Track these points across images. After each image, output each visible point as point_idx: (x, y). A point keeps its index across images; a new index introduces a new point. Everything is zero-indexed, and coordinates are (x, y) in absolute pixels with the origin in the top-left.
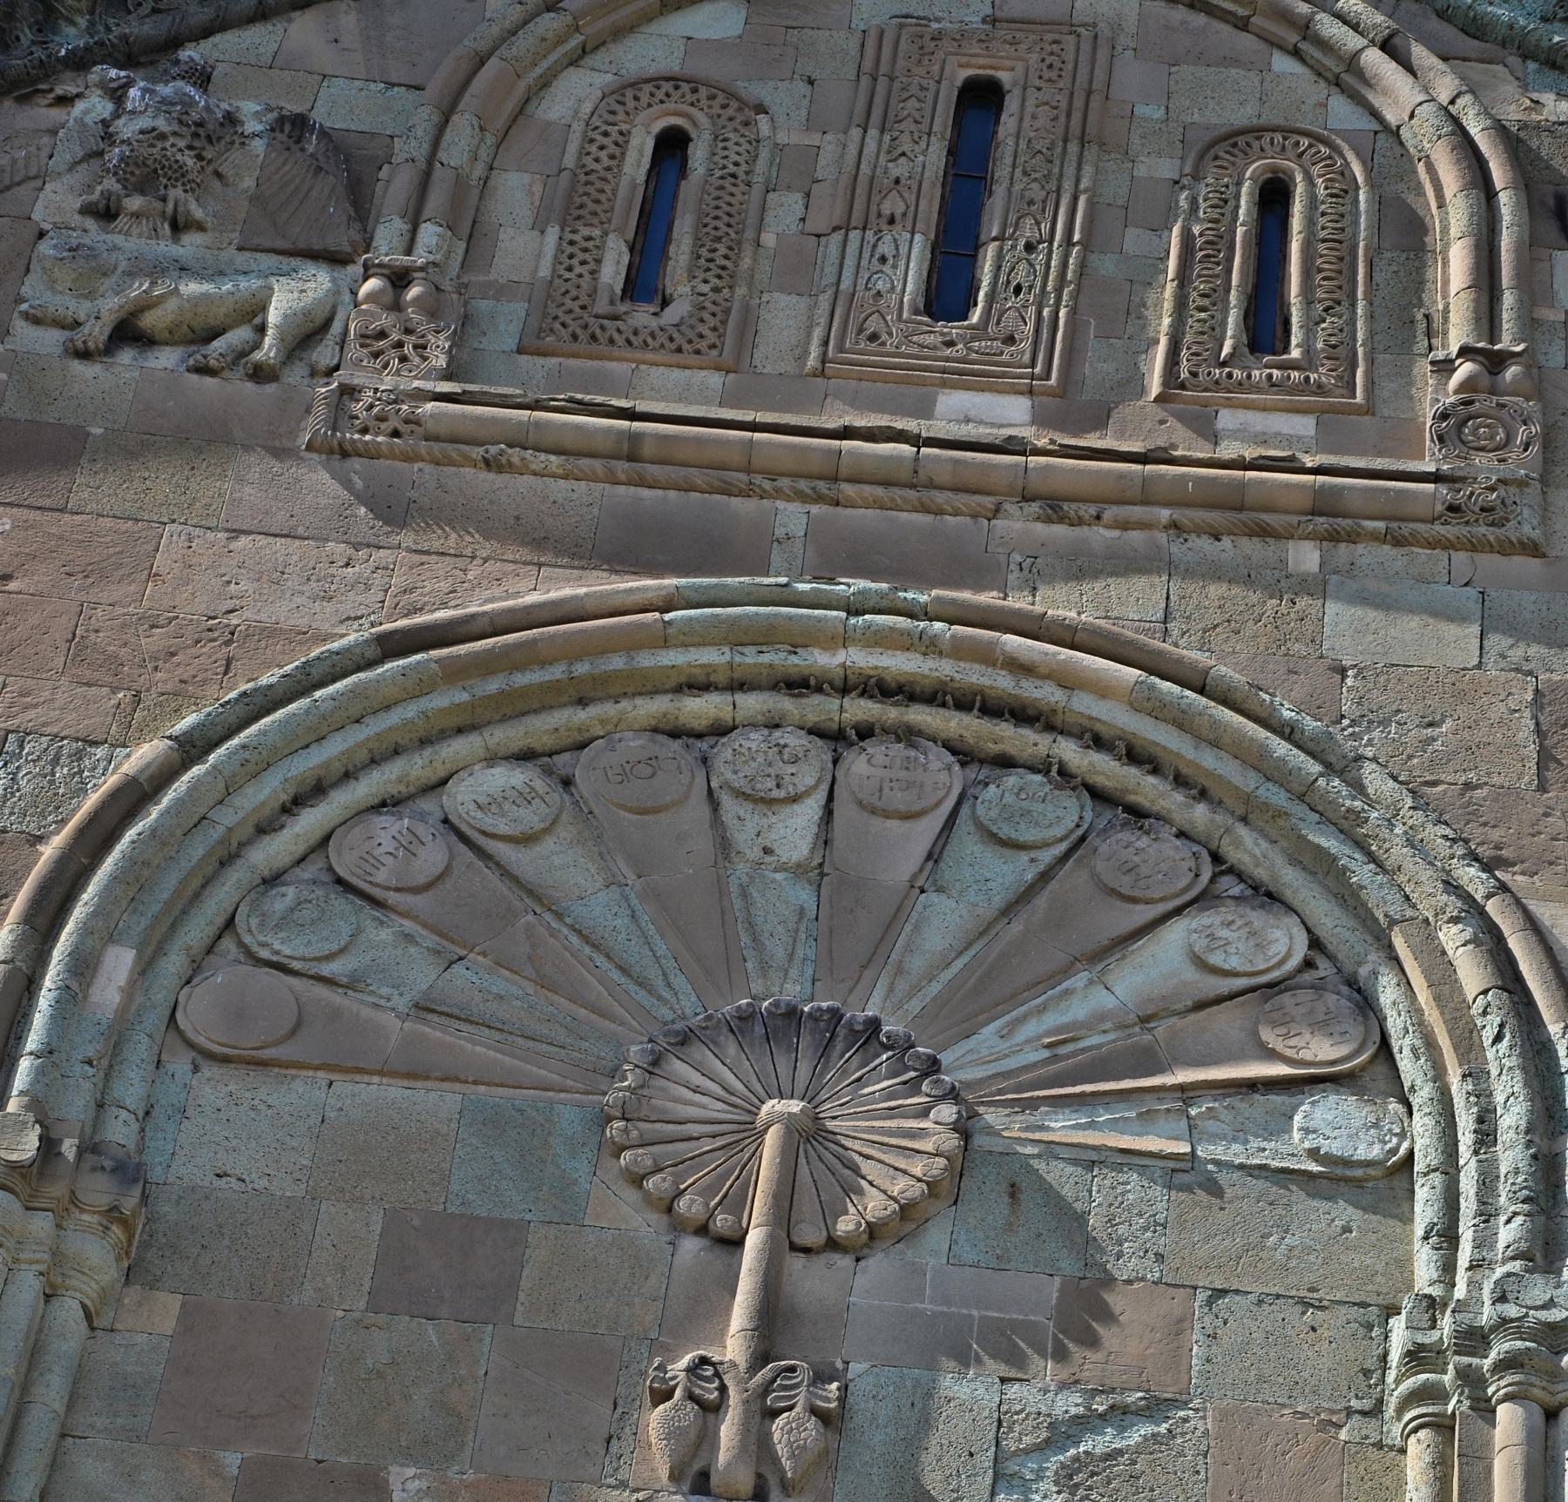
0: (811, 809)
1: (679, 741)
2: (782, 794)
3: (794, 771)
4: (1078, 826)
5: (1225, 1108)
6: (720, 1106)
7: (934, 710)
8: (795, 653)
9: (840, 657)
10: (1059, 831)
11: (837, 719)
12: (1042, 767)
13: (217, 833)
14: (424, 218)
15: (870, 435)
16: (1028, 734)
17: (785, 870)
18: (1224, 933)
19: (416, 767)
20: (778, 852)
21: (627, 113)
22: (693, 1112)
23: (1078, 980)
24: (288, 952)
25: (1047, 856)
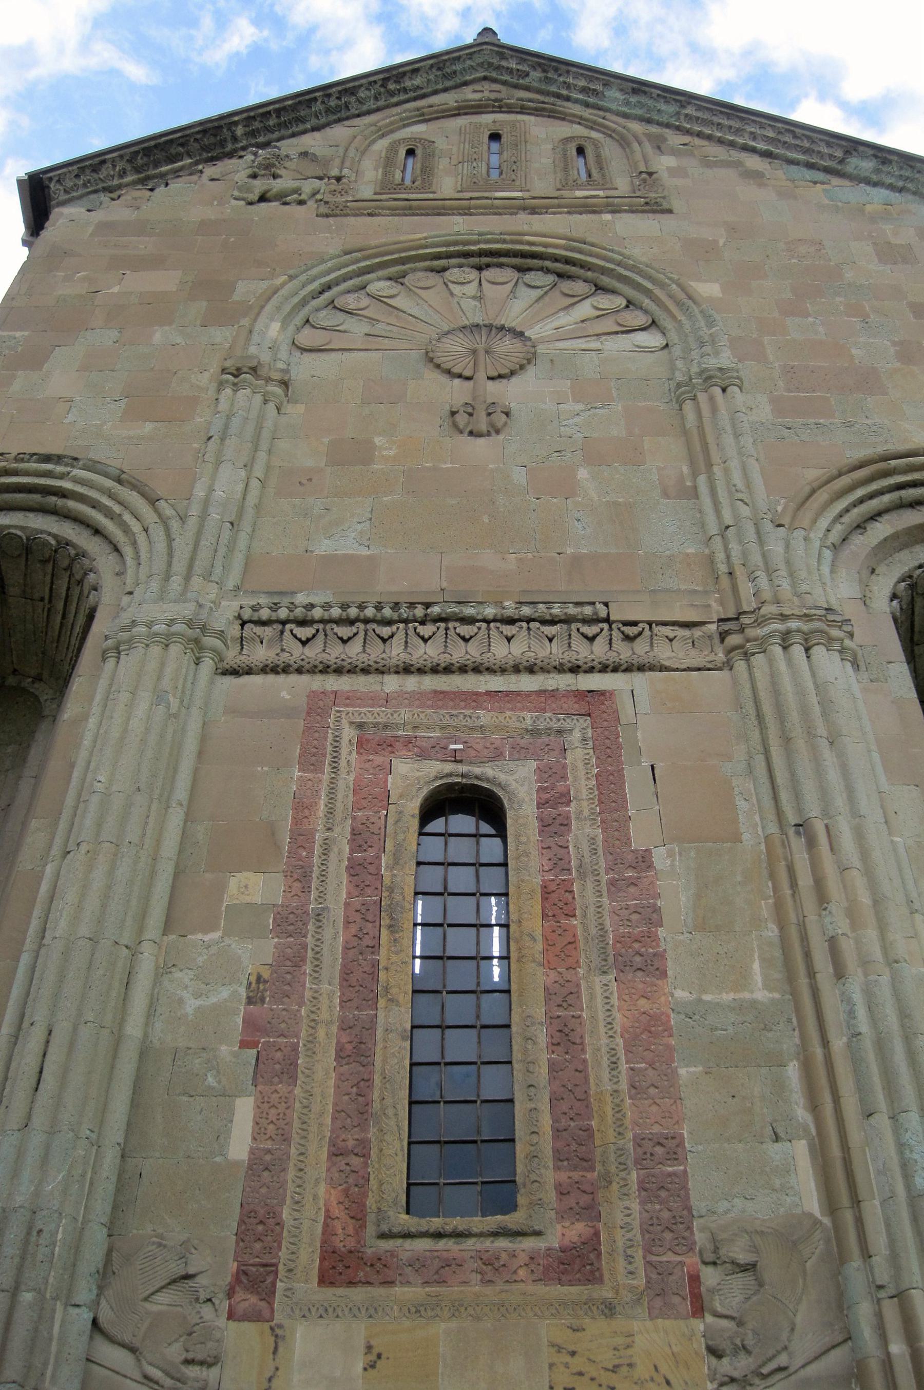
0: (476, 283)
9: (478, 247)
12: (541, 269)
15: (477, 198)
16: (535, 261)
25: (545, 289)
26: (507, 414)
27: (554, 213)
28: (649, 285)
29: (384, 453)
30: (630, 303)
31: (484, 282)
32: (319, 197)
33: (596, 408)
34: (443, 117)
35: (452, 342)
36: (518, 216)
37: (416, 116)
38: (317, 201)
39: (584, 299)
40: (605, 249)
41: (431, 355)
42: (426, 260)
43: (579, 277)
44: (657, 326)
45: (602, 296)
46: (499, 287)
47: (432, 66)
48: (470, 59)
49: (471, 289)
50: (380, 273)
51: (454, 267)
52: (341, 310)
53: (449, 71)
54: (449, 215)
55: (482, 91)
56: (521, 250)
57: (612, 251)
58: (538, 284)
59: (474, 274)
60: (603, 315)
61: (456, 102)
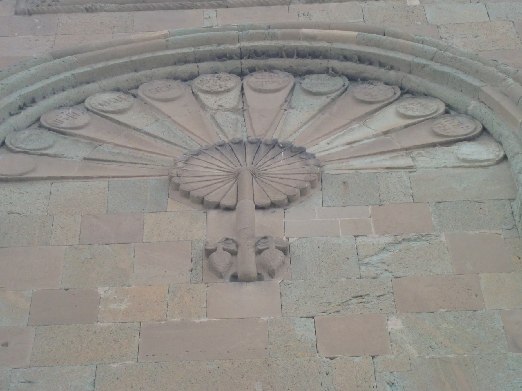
0: (236, 92)
2: (223, 89)
3: (226, 83)
4: (344, 86)
7: (278, 59)
8: (219, 46)
9: (238, 45)
10: (337, 88)
11: (240, 67)
12: (326, 71)
16: (318, 61)
17: (228, 111)
18: (411, 106)
19: (71, 94)
20: (224, 106)
25: (333, 96)
26: (285, 251)
28: (476, 83)
29: (113, 306)
30: (449, 109)
31: (247, 91)
33: (409, 240)
35: (205, 165)
40: (413, 40)
41: (176, 180)
42: (166, 65)
43: (377, 79)
44: (489, 133)
46: (271, 96)
50: (104, 83)
52: (50, 130)
54: (197, 8)
56: (296, 48)
58: (322, 89)
59: (233, 82)
60: (414, 124)
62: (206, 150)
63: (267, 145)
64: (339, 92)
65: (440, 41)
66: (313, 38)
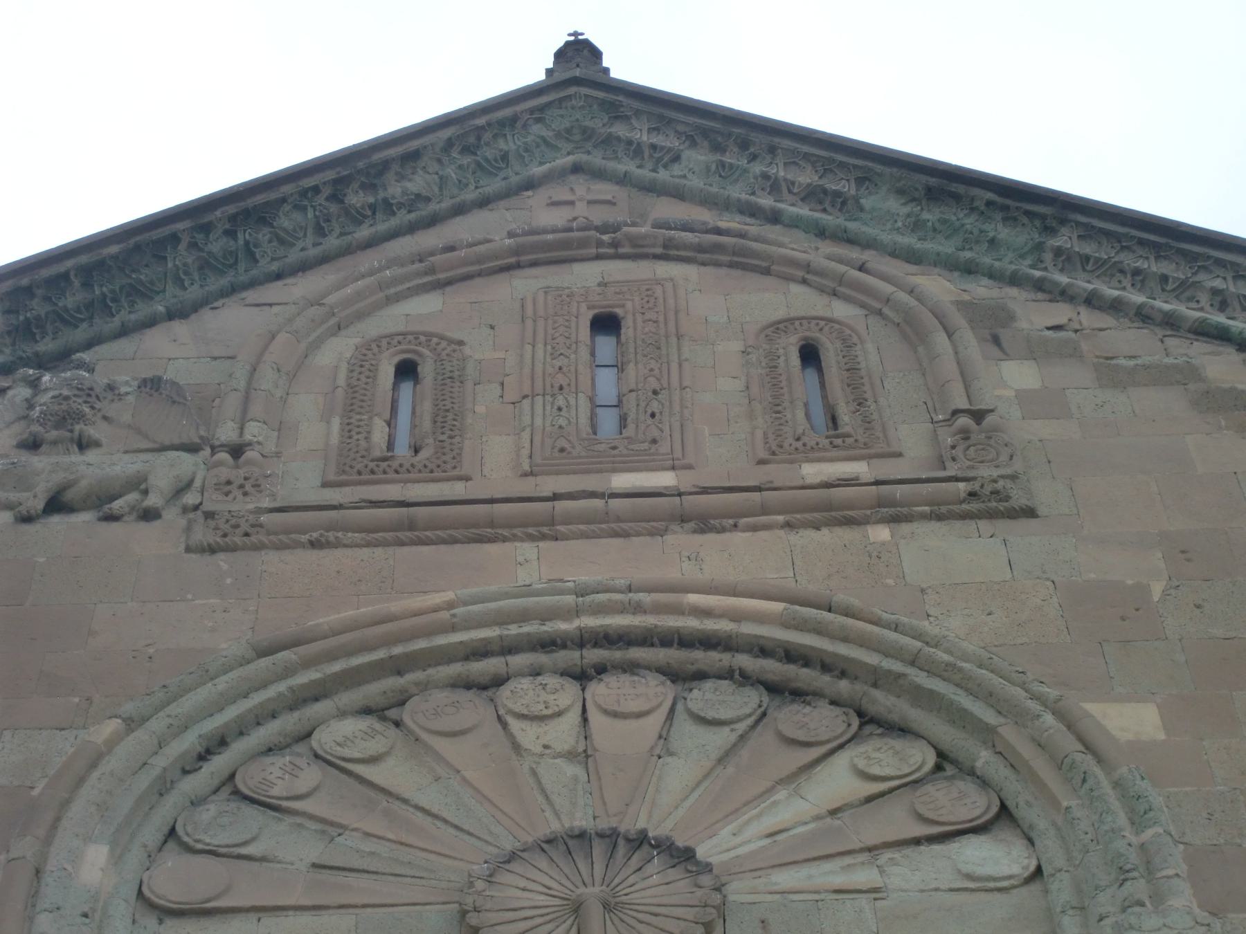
0: (573, 717)
1: (472, 691)
3: (555, 697)
4: (760, 706)
5: (902, 857)
6: (543, 897)
7: (646, 649)
8: (544, 624)
9: (576, 623)
10: (747, 710)
11: (579, 663)
13: (156, 772)
14: (249, 418)
15: (571, 496)
16: (714, 655)
17: (561, 757)
18: (877, 755)
19: (288, 722)
20: (552, 746)
21: (374, 355)
22: (526, 904)
23: (781, 794)
24: (216, 843)
25: (742, 727)
27: (755, 528)
31: (594, 716)
32: (190, 498)
34: (480, 274)
35: (523, 883)
36: (669, 538)
37: (419, 274)
38: (185, 510)
39: (832, 752)
42: (450, 660)
43: (818, 694)
45: (876, 742)
46: (633, 724)
47: (450, 144)
48: (539, 120)
49: (563, 732)
51: (521, 674)
53: (489, 153)
55: (572, 203)
56: (678, 631)
57: (896, 628)
58: (724, 714)
59: (566, 694)
61: (511, 235)
62: (523, 851)
63: (628, 840)
64: (753, 719)
65: (926, 623)
66: (706, 613)
